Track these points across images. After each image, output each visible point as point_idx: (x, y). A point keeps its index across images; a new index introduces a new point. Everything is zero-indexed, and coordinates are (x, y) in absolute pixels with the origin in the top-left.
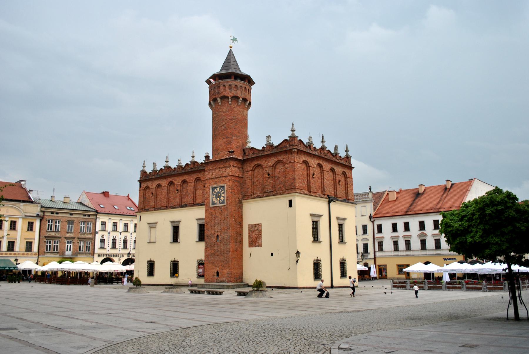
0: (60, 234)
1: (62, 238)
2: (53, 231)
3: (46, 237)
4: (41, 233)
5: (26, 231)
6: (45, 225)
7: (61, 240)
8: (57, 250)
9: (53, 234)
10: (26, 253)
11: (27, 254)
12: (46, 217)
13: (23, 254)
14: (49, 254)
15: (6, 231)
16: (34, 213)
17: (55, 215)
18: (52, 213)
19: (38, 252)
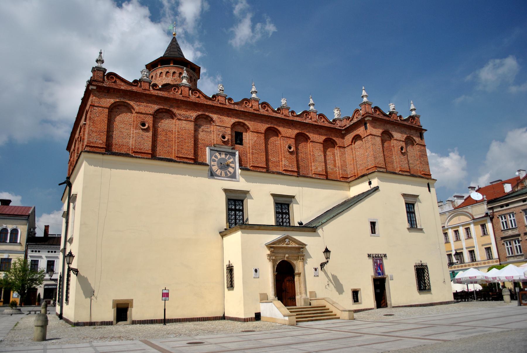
0: (517, 231)
1: (522, 235)
2: (510, 229)
3: (502, 238)
4: (496, 235)
5: (481, 236)
6: (498, 223)
7: (521, 238)
8: (521, 252)
9: (510, 233)
10: (486, 261)
11: (489, 263)
12: (495, 213)
13: (485, 263)
14: (512, 258)
15: (463, 240)
16: (482, 214)
17: (505, 208)
18: (502, 206)
19: (499, 258)
